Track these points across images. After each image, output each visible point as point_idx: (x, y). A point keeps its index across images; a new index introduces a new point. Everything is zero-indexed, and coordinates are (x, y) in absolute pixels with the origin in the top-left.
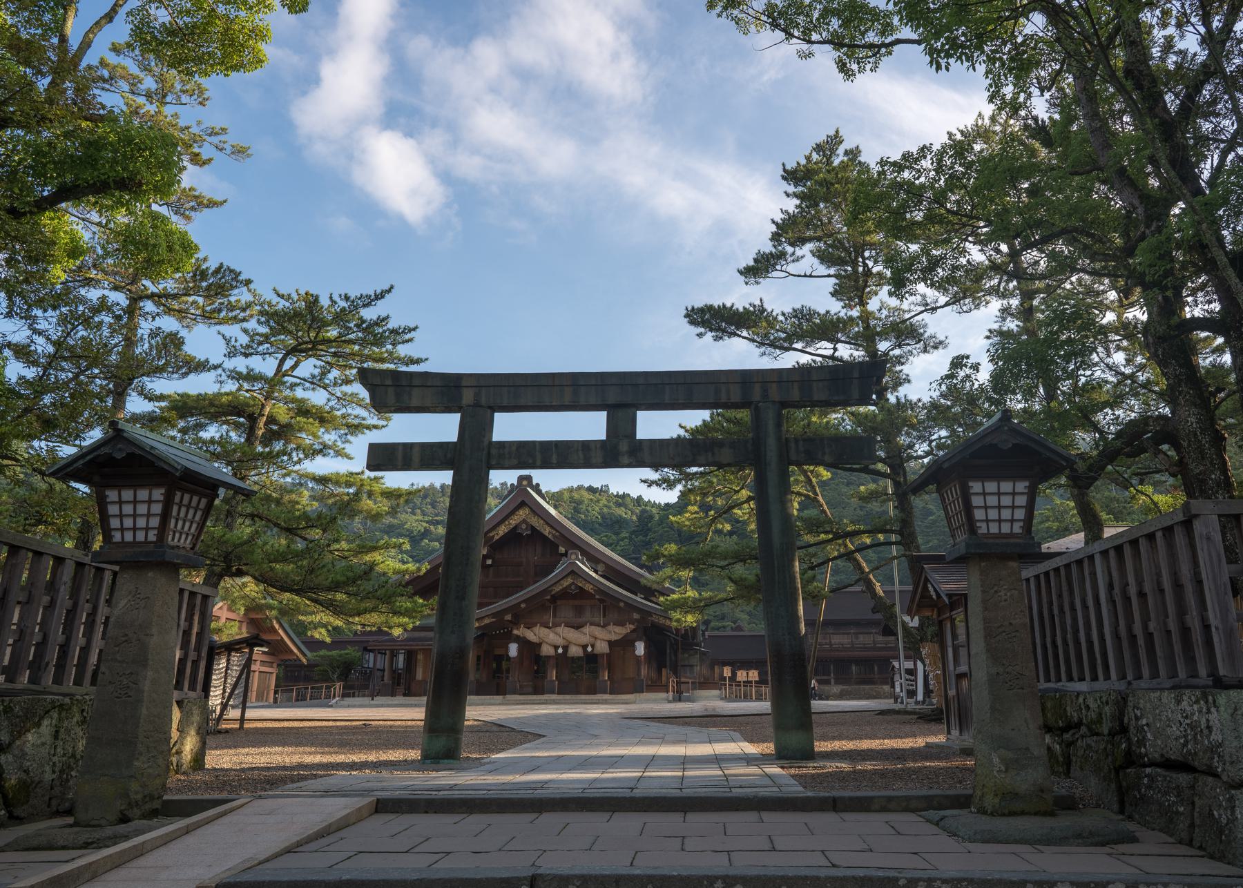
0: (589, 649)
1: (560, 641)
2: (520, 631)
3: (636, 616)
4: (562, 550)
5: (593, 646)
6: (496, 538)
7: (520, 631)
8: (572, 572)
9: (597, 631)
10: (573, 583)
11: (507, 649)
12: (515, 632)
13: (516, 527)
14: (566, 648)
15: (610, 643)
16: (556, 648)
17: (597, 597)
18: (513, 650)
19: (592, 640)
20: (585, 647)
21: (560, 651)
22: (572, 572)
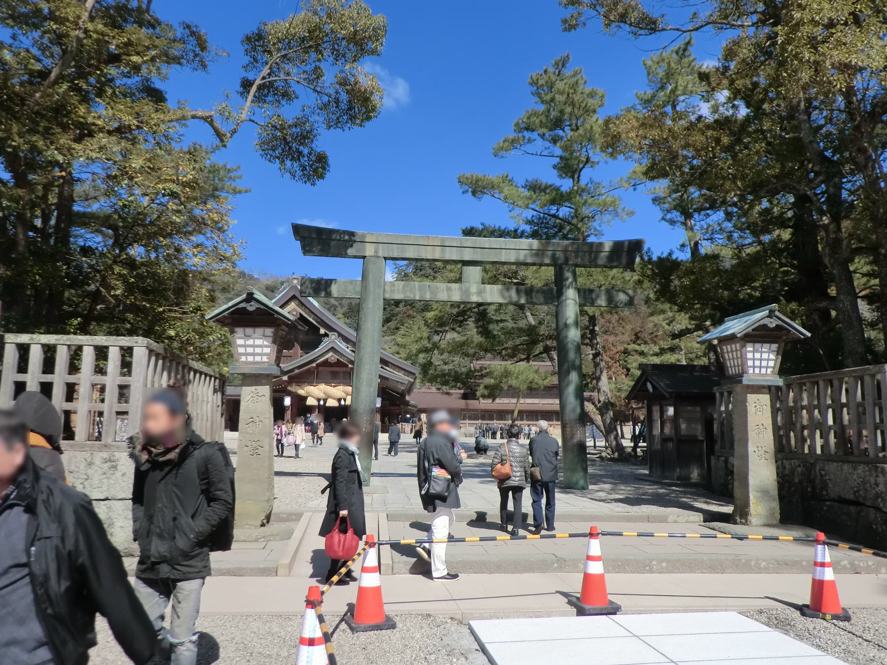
1: (322, 395)
2: (293, 388)
4: (322, 331)
7: (293, 388)
8: (332, 349)
10: (332, 356)
12: (289, 388)
14: (325, 401)
16: (319, 400)
20: (339, 400)
21: (322, 403)
22: (332, 349)
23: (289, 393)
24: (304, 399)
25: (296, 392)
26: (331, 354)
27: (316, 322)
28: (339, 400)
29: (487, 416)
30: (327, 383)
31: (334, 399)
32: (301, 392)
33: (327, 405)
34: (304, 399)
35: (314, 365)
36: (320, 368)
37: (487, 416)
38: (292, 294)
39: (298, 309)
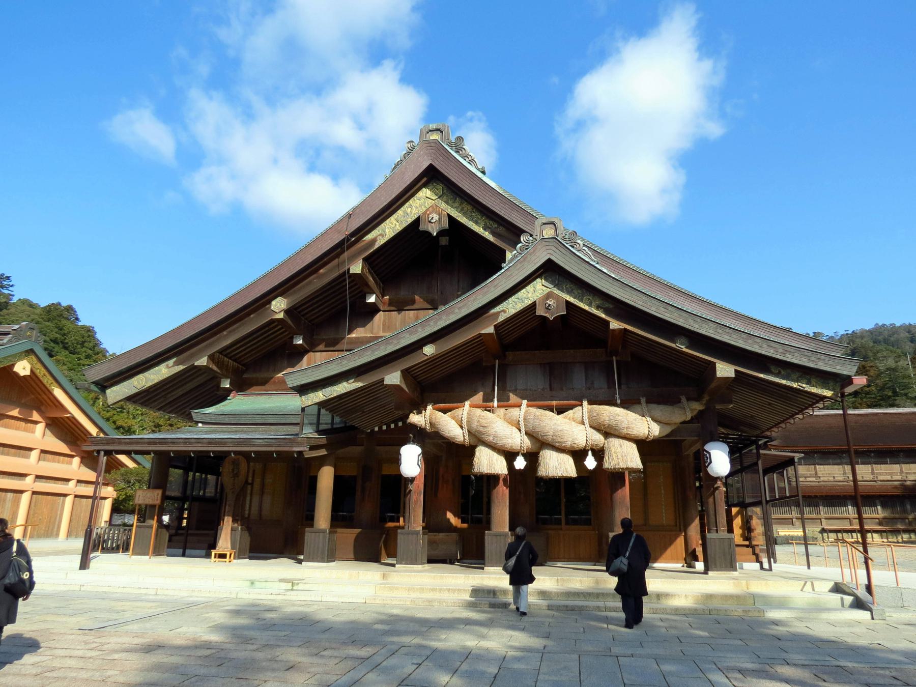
0: (590, 463)
3: (725, 370)
5: (599, 454)
6: (381, 242)
8: (550, 270)
10: (549, 296)
11: (397, 460)
12: (415, 419)
13: (417, 221)
14: (532, 458)
15: (644, 445)
16: (510, 456)
17: (615, 325)
19: (598, 438)
20: (578, 455)
21: (520, 463)
23: (419, 435)
24: (465, 452)
26: (537, 290)
27: (493, 233)
28: (578, 455)
30: (535, 398)
34: (465, 452)
38: (425, 165)
39: (443, 205)
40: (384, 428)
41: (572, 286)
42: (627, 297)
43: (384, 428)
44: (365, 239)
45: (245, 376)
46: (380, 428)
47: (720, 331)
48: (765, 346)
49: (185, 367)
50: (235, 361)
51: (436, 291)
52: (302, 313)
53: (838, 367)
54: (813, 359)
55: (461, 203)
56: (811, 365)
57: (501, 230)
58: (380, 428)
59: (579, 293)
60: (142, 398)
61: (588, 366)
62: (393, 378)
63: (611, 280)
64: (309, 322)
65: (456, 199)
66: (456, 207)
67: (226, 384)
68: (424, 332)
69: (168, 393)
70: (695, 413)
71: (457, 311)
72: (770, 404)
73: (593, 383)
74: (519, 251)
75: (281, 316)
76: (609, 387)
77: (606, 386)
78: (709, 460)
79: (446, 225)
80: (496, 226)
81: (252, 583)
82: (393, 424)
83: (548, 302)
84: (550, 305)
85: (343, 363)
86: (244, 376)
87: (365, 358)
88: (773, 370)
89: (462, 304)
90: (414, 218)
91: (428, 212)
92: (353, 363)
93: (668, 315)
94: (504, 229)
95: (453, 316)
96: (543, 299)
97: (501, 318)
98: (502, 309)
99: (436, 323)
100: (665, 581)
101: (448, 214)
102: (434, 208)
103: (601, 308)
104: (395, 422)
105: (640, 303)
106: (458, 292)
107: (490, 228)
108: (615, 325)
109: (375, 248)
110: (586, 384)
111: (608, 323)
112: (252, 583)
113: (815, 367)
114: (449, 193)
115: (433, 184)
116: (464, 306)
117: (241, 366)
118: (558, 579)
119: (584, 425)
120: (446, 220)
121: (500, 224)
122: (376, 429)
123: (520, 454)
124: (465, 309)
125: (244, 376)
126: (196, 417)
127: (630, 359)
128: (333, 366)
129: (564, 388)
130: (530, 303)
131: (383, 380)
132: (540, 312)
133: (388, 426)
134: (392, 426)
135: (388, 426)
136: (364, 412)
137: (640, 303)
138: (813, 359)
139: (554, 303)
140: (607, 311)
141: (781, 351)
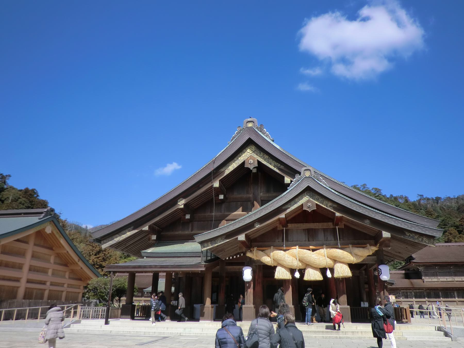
2: (253, 255)
3: (386, 234)
5: (332, 270)
7: (253, 255)
8: (309, 190)
9: (338, 252)
10: (308, 201)
12: (249, 255)
13: (243, 163)
14: (302, 272)
16: (292, 271)
17: (338, 214)
18: (248, 274)
20: (323, 271)
25: (259, 261)
26: (305, 199)
27: (279, 169)
28: (323, 271)
29: (432, 293)
31: (315, 268)
32: (267, 260)
33: (306, 278)
34: (273, 269)
35: (282, 216)
36: (290, 226)
37: (432, 293)
38: (247, 138)
39: (255, 156)
40: (231, 258)
41: (318, 197)
42: (343, 202)
43: (231, 258)
44: (220, 171)
45: (162, 233)
46: (229, 258)
47: (383, 218)
48: (403, 224)
49: (138, 231)
50: (158, 227)
51: (250, 193)
52: (190, 205)
53: (434, 234)
54: (424, 230)
55: (264, 155)
56: (423, 233)
57: (282, 167)
58: (229, 258)
59: (321, 200)
60: (117, 246)
61: (325, 230)
62: (242, 237)
63: (336, 195)
64: (192, 208)
65: (261, 153)
66: (261, 157)
67: (154, 237)
68: (255, 217)
69: (126, 243)
70: (374, 251)
71: (269, 208)
72: (407, 248)
73: (327, 238)
74: (295, 182)
75: (182, 206)
76: (335, 240)
77: (333, 240)
78: (380, 273)
79: (256, 165)
80: (280, 165)
81: (185, 329)
82: (235, 256)
83: (308, 204)
84: (309, 206)
85: (220, 231)
86: (161, 234)
87: (230, 229)
88: (407, 234)
89: (271, 205)
90: (242, 161)
91: (248, 159)
92: (225, 231)
93: (361, 210)
94: (283, 167)
95: (268, 210)
96: (306, 203)
97: (288, 211)
98: (288, 207)
99: (260, 213)
100: (364, 326)
101: (258, 160)
102: (251, 157)
103: (332, 207)
104: (236, 255)
105: (349, 205)
106: (261, 193)
107: (277, 166)
108: (338, 214)
109: (225, 175)
110: (324, 238)
111: (334, 214)
112: (185, 329)
113: (425, 233)
114: (258, 150)
115: (250, 146)
116: (272, 206)
117: (160, 229)
118: (317, 326)
119: (325, 257)
120: (256, 162)
121: (281, 164)
122: (227, 258)
123: (297, 270)
124: (273, 207)
125: (161, 234)
126: (143, 254)
127: (344, 227)
128: (217, 233)
129: (314, 240)
130: (300, 204)
131: (237, 238)
132: (305, 208)
133: (233, 257)
134: (235, 257)
135: (233, 257)
136: (225, 251)
137: (349, 205)
138: (424, 230)
139: (311, 204)
140: (334, 208)
141: (410, 226)
